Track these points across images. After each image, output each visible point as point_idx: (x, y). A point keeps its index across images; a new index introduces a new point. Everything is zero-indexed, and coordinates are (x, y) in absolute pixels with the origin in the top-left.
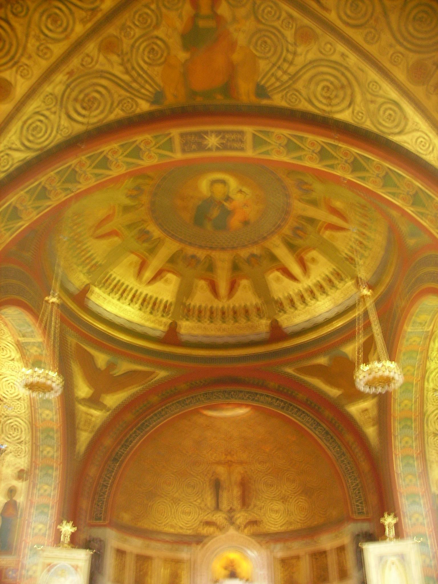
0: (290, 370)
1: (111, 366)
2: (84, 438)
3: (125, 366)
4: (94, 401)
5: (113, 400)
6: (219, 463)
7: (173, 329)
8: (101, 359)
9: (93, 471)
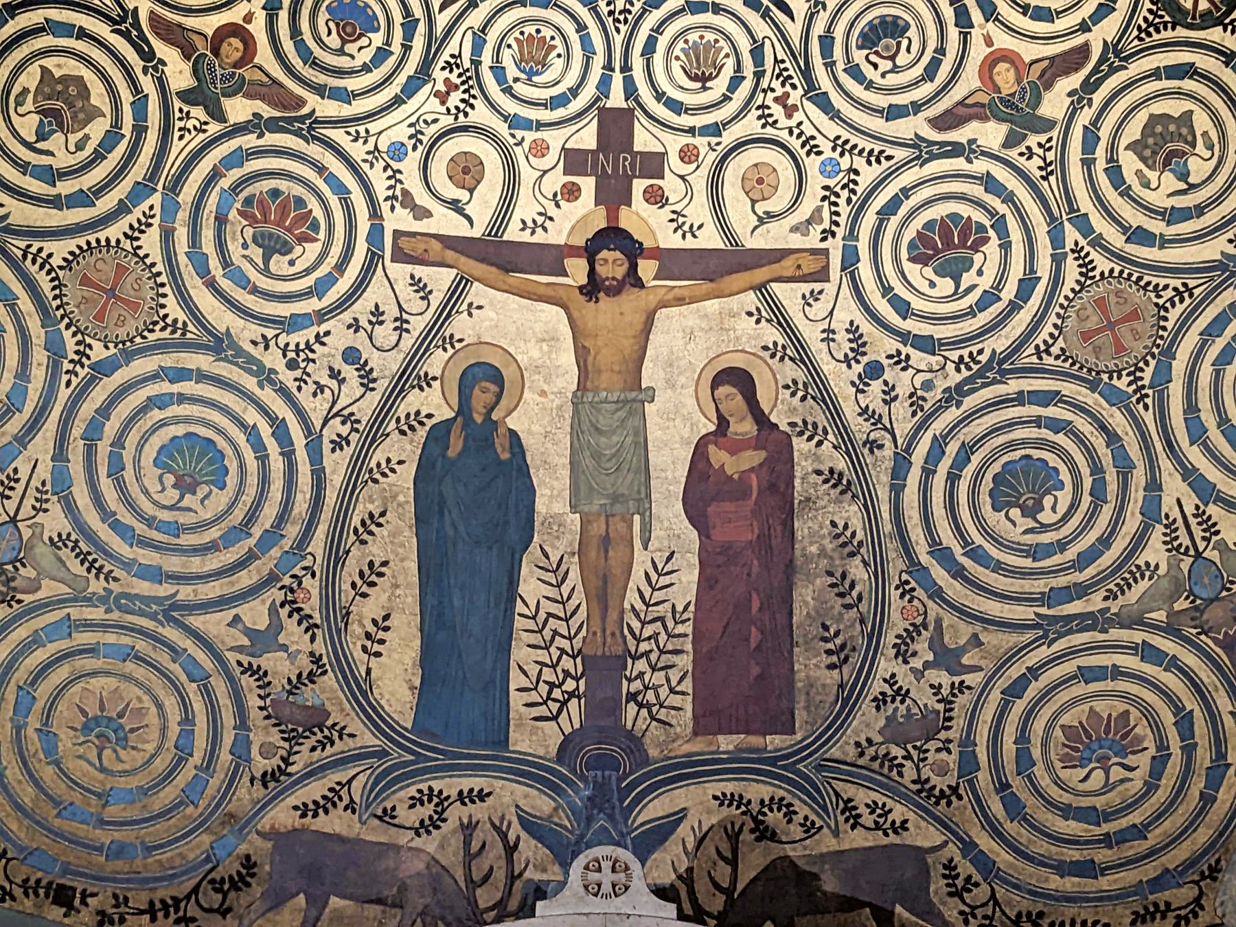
6: (498, 257)
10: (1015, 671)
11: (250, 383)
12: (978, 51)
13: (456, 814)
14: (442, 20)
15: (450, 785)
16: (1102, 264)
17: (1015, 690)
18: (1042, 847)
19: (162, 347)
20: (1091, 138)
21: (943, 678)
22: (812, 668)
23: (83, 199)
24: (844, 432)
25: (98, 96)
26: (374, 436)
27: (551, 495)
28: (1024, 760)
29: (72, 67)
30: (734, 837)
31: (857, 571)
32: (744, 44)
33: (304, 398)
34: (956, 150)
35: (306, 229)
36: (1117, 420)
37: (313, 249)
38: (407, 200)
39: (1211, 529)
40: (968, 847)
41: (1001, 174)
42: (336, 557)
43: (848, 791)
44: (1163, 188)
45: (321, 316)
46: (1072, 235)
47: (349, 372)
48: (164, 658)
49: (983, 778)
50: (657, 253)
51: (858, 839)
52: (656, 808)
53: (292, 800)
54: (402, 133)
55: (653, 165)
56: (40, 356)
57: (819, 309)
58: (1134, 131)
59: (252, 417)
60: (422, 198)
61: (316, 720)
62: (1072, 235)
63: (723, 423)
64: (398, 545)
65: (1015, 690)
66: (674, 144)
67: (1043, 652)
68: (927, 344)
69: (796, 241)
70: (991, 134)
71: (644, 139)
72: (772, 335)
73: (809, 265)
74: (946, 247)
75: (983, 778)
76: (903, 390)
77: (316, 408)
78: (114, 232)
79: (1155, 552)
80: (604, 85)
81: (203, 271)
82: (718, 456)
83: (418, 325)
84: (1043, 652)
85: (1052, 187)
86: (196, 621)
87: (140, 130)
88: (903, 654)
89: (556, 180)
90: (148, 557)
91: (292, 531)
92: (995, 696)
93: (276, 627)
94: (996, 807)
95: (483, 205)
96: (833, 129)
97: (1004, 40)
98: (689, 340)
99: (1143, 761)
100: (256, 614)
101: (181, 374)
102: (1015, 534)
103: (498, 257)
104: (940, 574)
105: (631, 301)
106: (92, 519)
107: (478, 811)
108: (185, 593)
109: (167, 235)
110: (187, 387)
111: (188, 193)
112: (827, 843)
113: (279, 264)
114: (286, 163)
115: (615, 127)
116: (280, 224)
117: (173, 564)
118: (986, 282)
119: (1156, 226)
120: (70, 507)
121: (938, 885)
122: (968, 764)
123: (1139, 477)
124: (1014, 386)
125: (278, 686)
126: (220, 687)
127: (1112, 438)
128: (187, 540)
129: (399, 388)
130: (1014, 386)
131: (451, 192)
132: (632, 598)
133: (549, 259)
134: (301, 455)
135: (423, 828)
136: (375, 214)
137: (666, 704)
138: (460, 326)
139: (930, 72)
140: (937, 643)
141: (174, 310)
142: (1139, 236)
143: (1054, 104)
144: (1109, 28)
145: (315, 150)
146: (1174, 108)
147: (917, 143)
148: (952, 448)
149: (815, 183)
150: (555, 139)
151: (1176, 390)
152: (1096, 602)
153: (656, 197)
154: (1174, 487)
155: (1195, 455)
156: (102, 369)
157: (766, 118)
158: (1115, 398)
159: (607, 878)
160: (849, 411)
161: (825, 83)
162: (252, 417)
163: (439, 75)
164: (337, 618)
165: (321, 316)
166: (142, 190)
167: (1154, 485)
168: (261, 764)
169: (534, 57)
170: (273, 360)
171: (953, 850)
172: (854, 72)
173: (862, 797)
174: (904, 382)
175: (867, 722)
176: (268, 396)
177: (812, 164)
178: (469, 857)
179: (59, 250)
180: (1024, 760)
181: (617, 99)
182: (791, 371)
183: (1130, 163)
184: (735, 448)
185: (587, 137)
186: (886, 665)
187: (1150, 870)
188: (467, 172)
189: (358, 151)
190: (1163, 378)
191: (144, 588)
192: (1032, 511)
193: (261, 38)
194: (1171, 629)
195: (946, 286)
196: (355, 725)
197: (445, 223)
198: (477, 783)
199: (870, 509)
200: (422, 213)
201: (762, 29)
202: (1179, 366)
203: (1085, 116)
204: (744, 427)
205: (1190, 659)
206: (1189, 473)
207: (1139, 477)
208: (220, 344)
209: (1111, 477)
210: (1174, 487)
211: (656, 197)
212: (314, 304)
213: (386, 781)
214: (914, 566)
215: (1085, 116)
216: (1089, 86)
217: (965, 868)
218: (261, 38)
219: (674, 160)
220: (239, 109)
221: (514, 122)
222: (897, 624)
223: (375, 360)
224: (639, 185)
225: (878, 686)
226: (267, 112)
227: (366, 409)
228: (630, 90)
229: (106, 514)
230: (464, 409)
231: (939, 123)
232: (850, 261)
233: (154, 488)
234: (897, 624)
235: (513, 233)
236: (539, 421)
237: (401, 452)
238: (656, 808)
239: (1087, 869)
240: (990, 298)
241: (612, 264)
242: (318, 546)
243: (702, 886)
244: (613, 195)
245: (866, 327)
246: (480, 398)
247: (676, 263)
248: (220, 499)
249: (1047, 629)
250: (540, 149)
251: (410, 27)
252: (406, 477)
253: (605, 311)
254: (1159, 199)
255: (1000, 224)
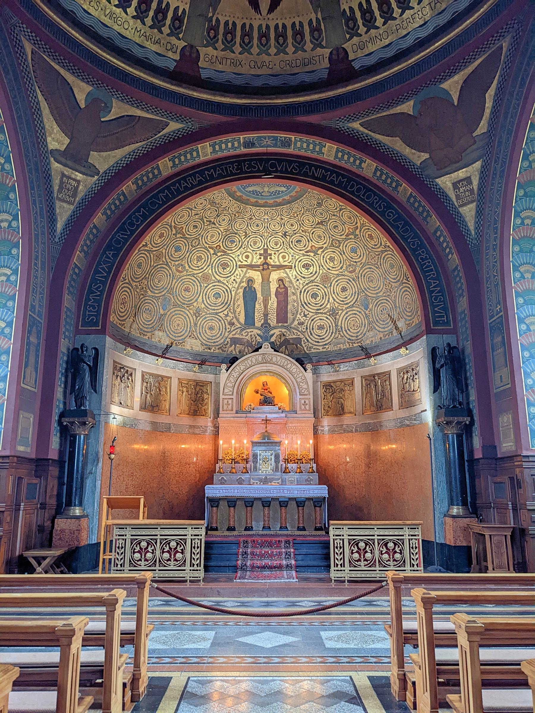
0: (356, 125)
1: (96, 105)
2: (64, 212)
3: (118, 109)
4: (75, 157)
5: (104, 160)
6: (251, 267)
7: (189, 56)
8: (82, 91)
9: (78, 258)
10: (312, 318)
11: (223, 285)
12: (310, 245)
13: (250, 334)
14: (243, 240)
15: (249, 330)
16: (325, 272)
17: (312, 320)
18: (314, 339)
19: (212, 283)
20: (323, 257)
21: (305, 318)
22: (290, 315)
23: (202, 268)
24: (294, 287)
25: (203, 257)
26: (238, 289)
27: (259, 295)
28: (313, 329)
29: (200, 254)
30: (281, 336)
31: (295, 304)
32: (282, 242)
33: (229, 286)
34: (308, 255)
35: (228, 266)
36: (325, 290)
37: (229, 268)
38: (240, 261)
39: (335, 304)
40: (306, 338)
41: (313, 259)
42: (234, 304)
43: (294, 331)
44: (331, 264)
45: (230, 276)
46: (321, 267)
47: (234, 282)
48: (216, 319)
49: (308, 330)
50: (271, 265)
51: (294, 336)
52: (272, 332)
53: (232, 334)
54: (239, 253)
55: (271, 255)
56: (199, 287)
57: (291, 272)
58: (328, 257)
59: (223, 289)
60: (242, 261)
61: (233, 324)
62: (321, 267)
63: (280, 286)
64: (241, 302)
65: (312, 320)
66: (273, 252)
67: (316, 316)
68: (304, 278)
69: (288, 264)
70: (312, 254)
71: (269, 252)
72: (285, 275)
73: (290, 267)
74: (307, 266)
75: (308, 330)
76: (301, 283)
77: (230, 287)
78: (206, 271)
79: (328, 306)
80: (264, 246)
81: (216, 273)
82: (279, 289)
83: (242, 275)
84: (316, 316)
85: (319, 262)
86: (219, 314)
87: (208, 259)
88: (300, 315)
89: (259, 257)
90: (213, 308)
91: (229, 302)
92: (310, 320)
93: (228, 314)
94: (309, 334)
95: (249, 261)
96: (293, 251)
97: (313, 244)
98: (275, 276)
99: (325, 330)
100: (226, 312)
101: (215, 286)
102: (313, 301)
103: (251, 267)
104: (305, 305)
105: (268, 270)
106: (207, 305)
107: (252, 333)
108: (218, 311)
109: (212, 270)
110: (215, 287)
111: (214, 265)
112: (291, 337)
113: (225, 270)
114: (225, 259)
115: (266, 251)
116: (225, 266)
117: (216, 308)
118: (311, 271)
119: (331, 268)
120: (204, 304)
121: (303, 342)
122: (307, 328)
123: (327, 297)
124: (314, 284)
125: (229, 320)
126: (222, 321)
127: (325, 292)
128: (217, 305)
129: (240, 283)
130: (314, 284)
131: (245, 259)
132: (269, 307)
133: (258, 266)
134: (229, 293)
135: (246, 336)
136: (236, 263)
137: (273, 320)
138: (247, 275)
139: (305, 246)
140: (304, 314)
141: (213, 278)
142: (329, 269)
143: (319, 252)
144: (325, 246)
145: (229, 257)
146: (333, 256)
147: (303, 254)
148: (307, 290)
149: (291, 257)
150: (258, 252)
151: (332, 287)
152: (322, 311)
153: (271, 258)
154: (331, 299)
155: (334, 296)
156: (206, 287)
157: (284, 250)
158: (325, 287)
159: (266, 347)
160: (295, 284)
161: (292, 246)
162: (223, 289)
163: (243, 246)
164: (235, 312)
165: (230, 276)
166: (208, 266)
167: (329, 298)
168: (228, 330)
169: (255, 243)
170: (225, 282)
171: (304, 339)
172: (295, 245)
173: (295, 331)
174: (301, 282)
175: (296, 323)
176: (225, 286)
177: (290, 255)
178: (251, 339)
179: (200, 275)
180: (313, 329)
181: (266, 247)
182: (287, 279)
183: (328, 261)
184: (281, 289)
185: (262, 252)
186: (298, 316)
187: (324, 343)
188: (247, 257)
189: (234, 256)
190: (331, 286)
191: (213, 311)
192: (315, 299)
193: (221, 246)
194: (329, 316)
195: (306, 271)
196: (238, 324)
197: (246, 263)
198: (252, 330)
199: (297, 296)
200: (242, 262)
201: (284, 240)
202: (332, 285)
203: (323, 254)
204: (282, 286)
205: (331, 319)
206: (333, 297)
207: (327, 297)
208: (219, 281)
209: (324, 296)
210: (331, 299)
211: (271, 258)
212: (229, 275)
213: (242, 330)
214: (303, 305)
215: (323, 254)
216: (323, 251)
217: (306, 341)
218: (221, 246)
219: (273, 254)
220: (219, 254)
221: (253, 251)
222: (300, 311)
223: (237, 280)
224: (269, 257)
225: (297, 318)
226: (223, 254)
227: (236, 286)
228: (267, 246)
229: (208, 304)
230: (248, 285)
231: (305, 252)
232: (295, 266)
233: (213, 299)
234: (300, 311)
235: (253, 263)
236: (257, 286)
237: (241, 291)
238: (272, 332)
239: (318, 342)
240: (311, 273)
241: (266, 266)
242: (232, 303)
243: (277, 342)
244: (266, 258)
245: (297, 275)
246: (250, 283)
247: (273, 266)
248: (220, 299)
249: (317, 313)
250: (256, 253)
251: (239, 242)
252: (241, 294)
253: (265, 272)
254: (331, 265)
255: (313, 265)
